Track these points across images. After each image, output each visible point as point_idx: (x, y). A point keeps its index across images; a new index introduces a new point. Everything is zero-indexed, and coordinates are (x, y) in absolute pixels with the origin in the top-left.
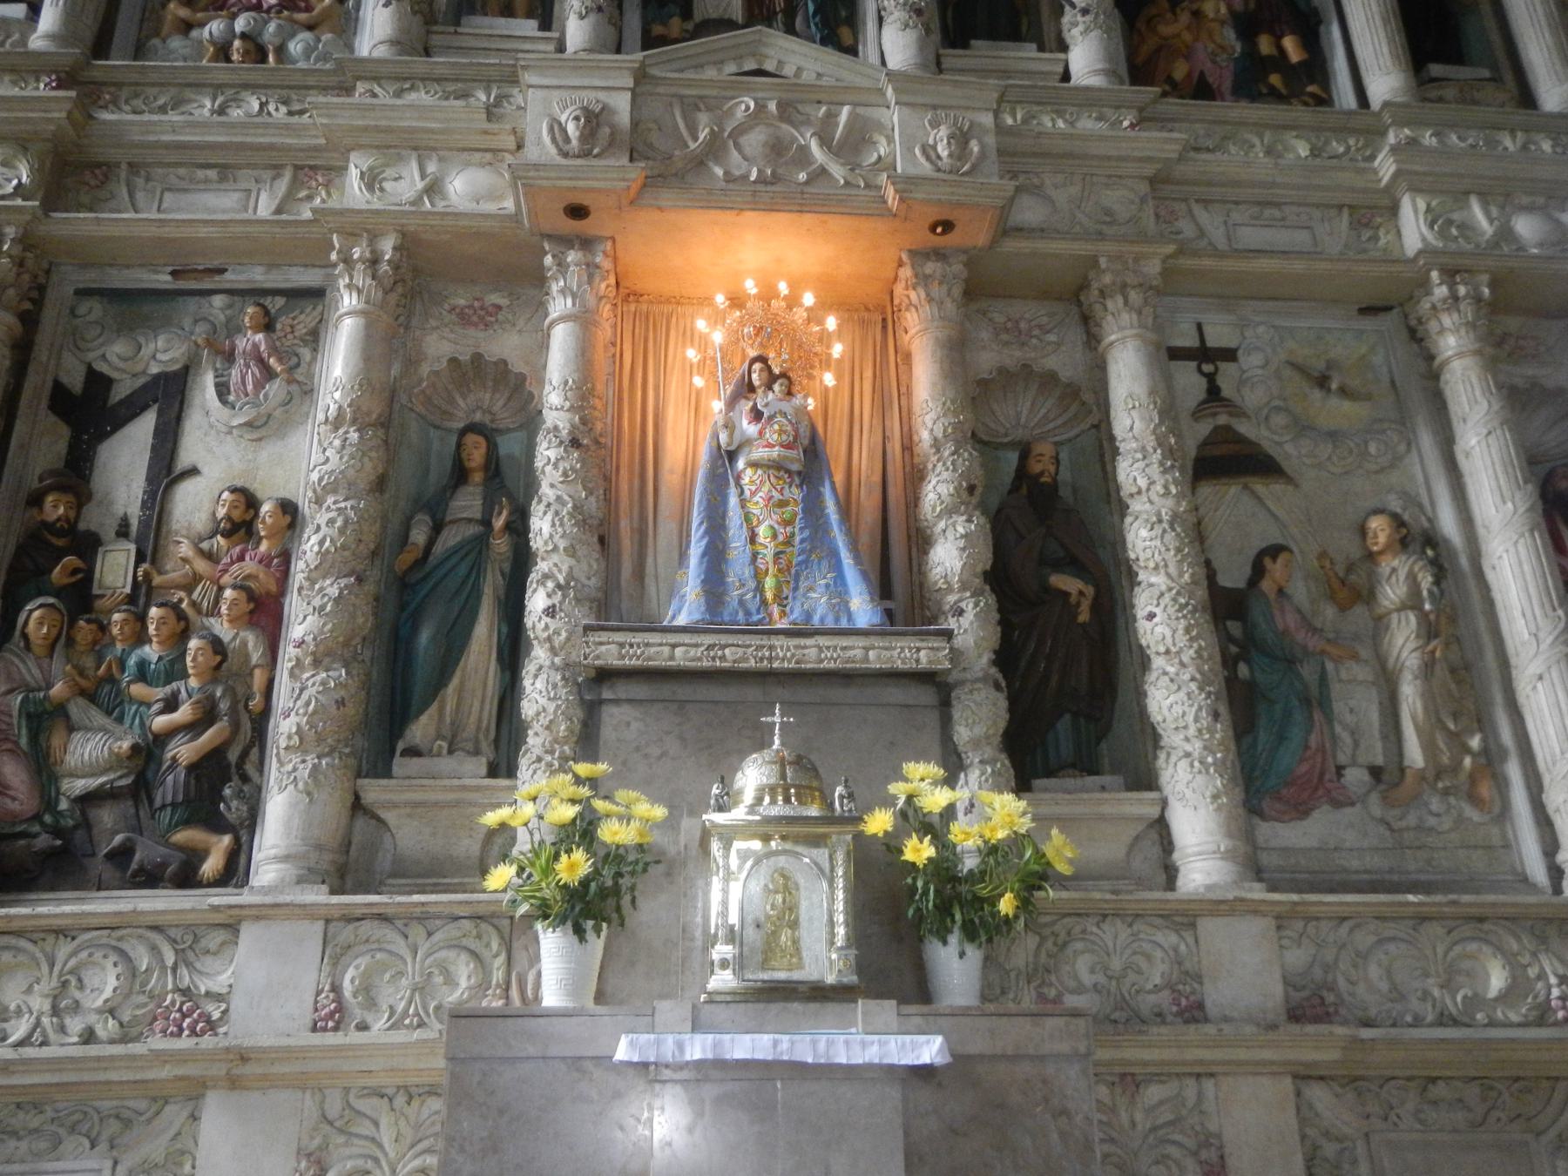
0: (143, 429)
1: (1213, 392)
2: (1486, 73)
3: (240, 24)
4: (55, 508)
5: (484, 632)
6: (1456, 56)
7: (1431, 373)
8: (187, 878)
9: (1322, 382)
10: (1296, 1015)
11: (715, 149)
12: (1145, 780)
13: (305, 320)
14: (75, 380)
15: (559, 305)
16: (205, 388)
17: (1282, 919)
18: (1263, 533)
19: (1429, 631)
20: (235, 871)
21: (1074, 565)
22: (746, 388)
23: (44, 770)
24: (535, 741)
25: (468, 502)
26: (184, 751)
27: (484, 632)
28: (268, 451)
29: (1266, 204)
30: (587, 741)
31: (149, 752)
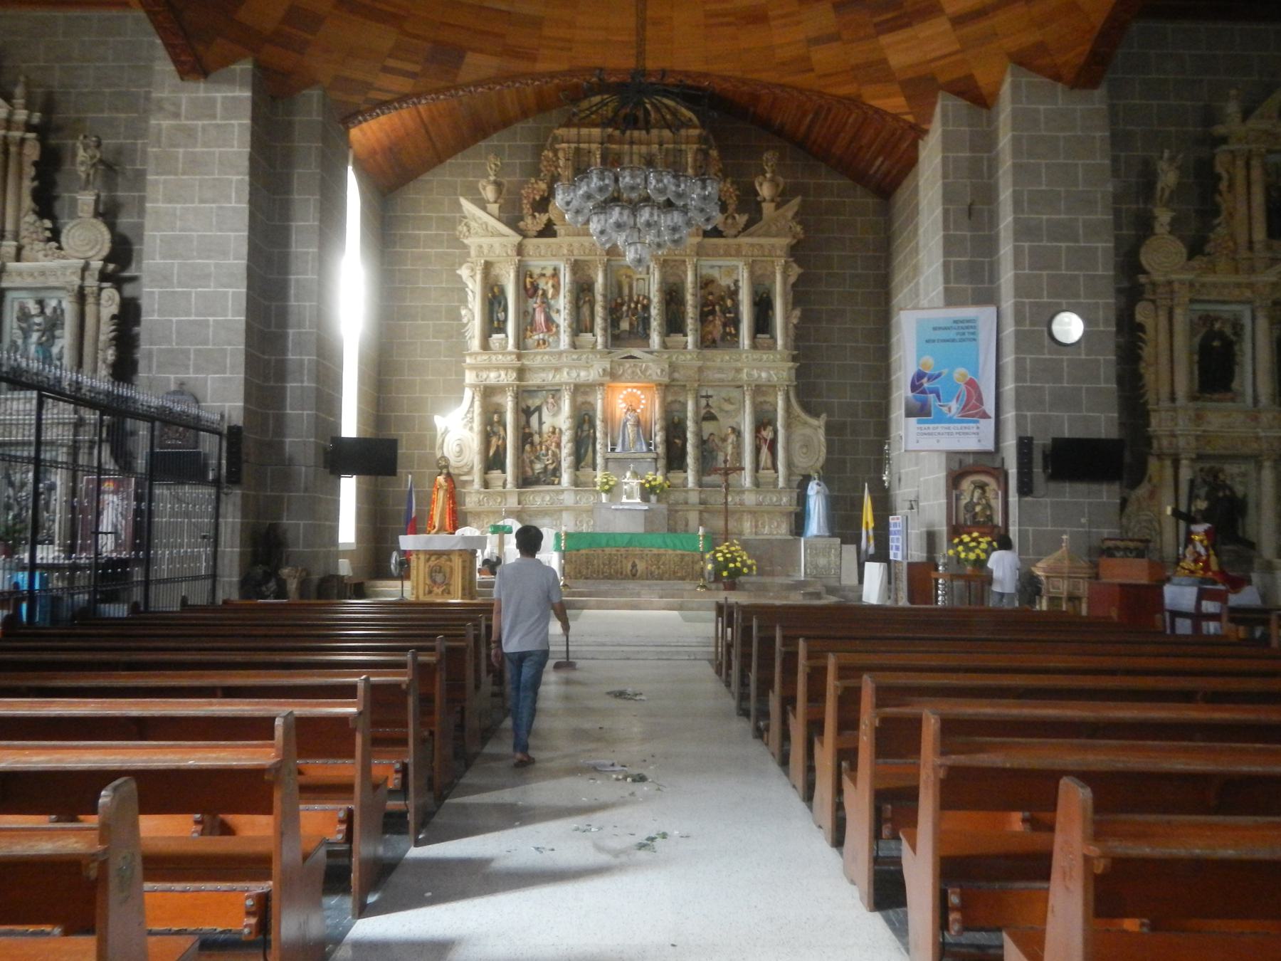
0: (536, 415)
1: (708, 405)
2: (768, 336)
3: (541, 336)
4: (527, 431)
5: (590, 449)
6: (763, 333)
7: (744, 401)
8: (553, 484)
9: (725, 400)
10: (701, 504)
11: (622, 374)
12: (686, 472)
13: (558, 396)
14: (525, 407)
15: (599, 396)
16: (545, 410)
17: (700, 492)
18: (711, 430)
19: (734, 448)
20: (559, 483)
21: (679, 438)
22: (628, 410)
23: (533, 469)
24: (599, 467)
25: (586, 427)
26: (551, 467)
27: (590, 449)
28: (555, 419)
29: (721, 370)
30: (606, 468)
31: (546, 466)
